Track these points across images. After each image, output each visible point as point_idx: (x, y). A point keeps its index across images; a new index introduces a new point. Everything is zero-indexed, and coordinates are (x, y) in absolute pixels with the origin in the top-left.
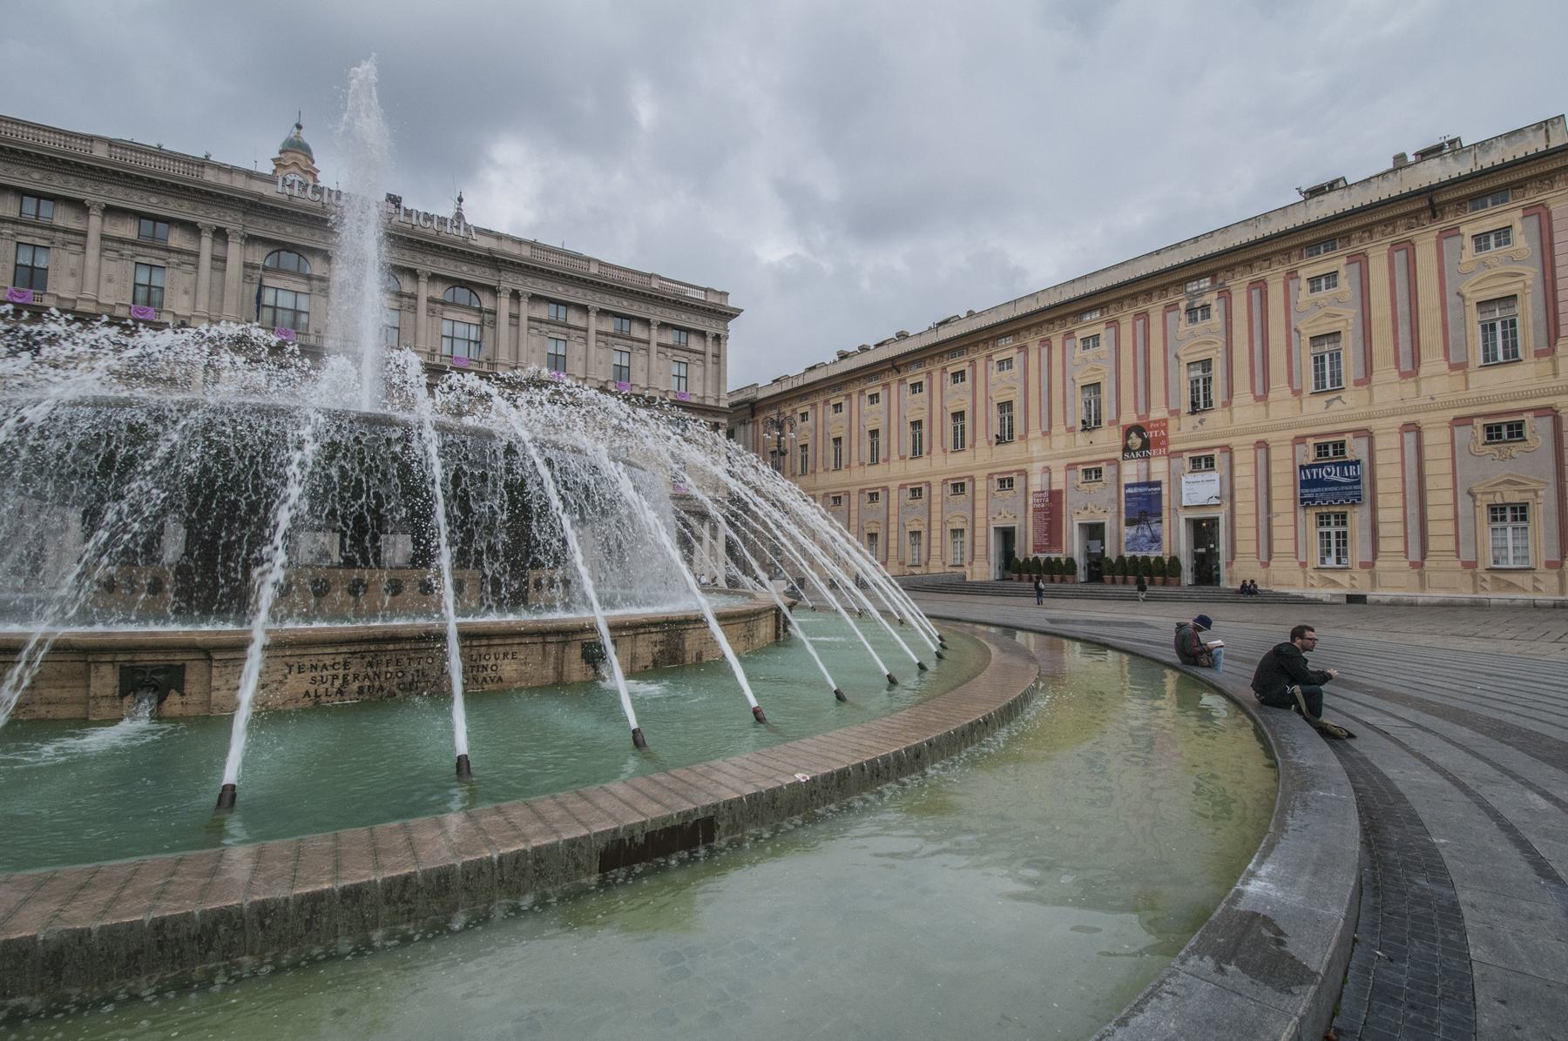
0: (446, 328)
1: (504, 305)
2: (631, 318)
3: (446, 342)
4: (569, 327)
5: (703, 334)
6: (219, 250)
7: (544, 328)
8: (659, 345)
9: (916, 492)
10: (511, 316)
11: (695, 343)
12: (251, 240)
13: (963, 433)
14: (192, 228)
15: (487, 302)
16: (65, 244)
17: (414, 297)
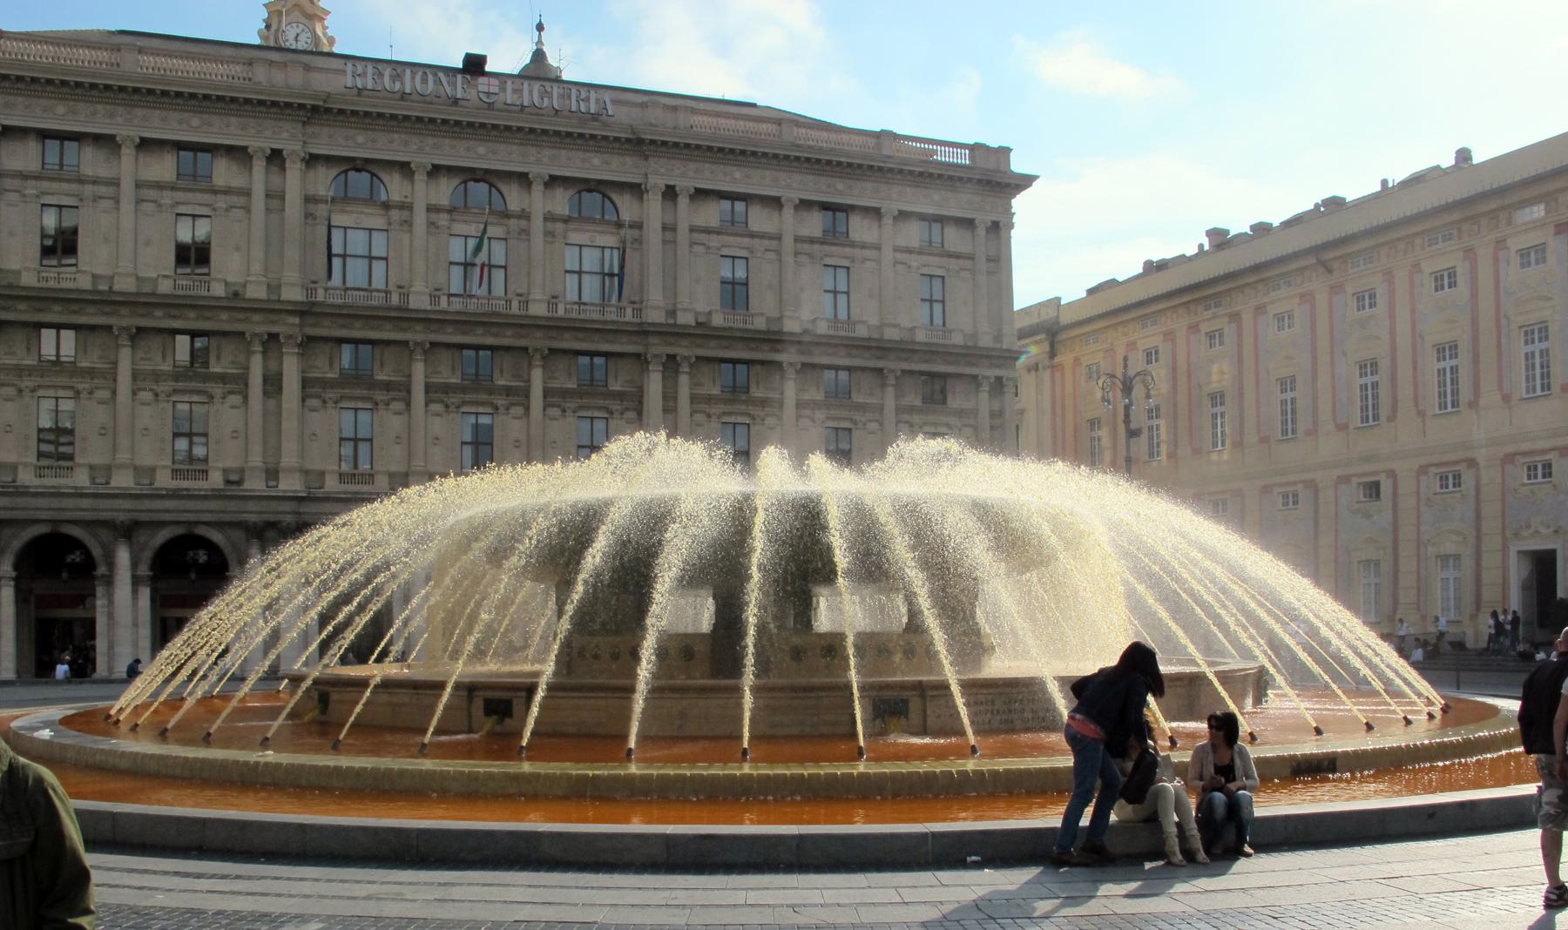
0: (571, 259)
1: (654, 210)
2: (847, 209)
3: (572, 281)
4: (752, 235)
5: (968, 223)
6: (276, 179)
7: (715, 241)
8: (896, 249)
9: (1373, 490)
10: (664, 228)
11: (954, 239)
12: (312, 160)
13: (1454, 381)
14: (239, 154)
15: (627, 208)
16: (97, 198)
17: (525, 215)
